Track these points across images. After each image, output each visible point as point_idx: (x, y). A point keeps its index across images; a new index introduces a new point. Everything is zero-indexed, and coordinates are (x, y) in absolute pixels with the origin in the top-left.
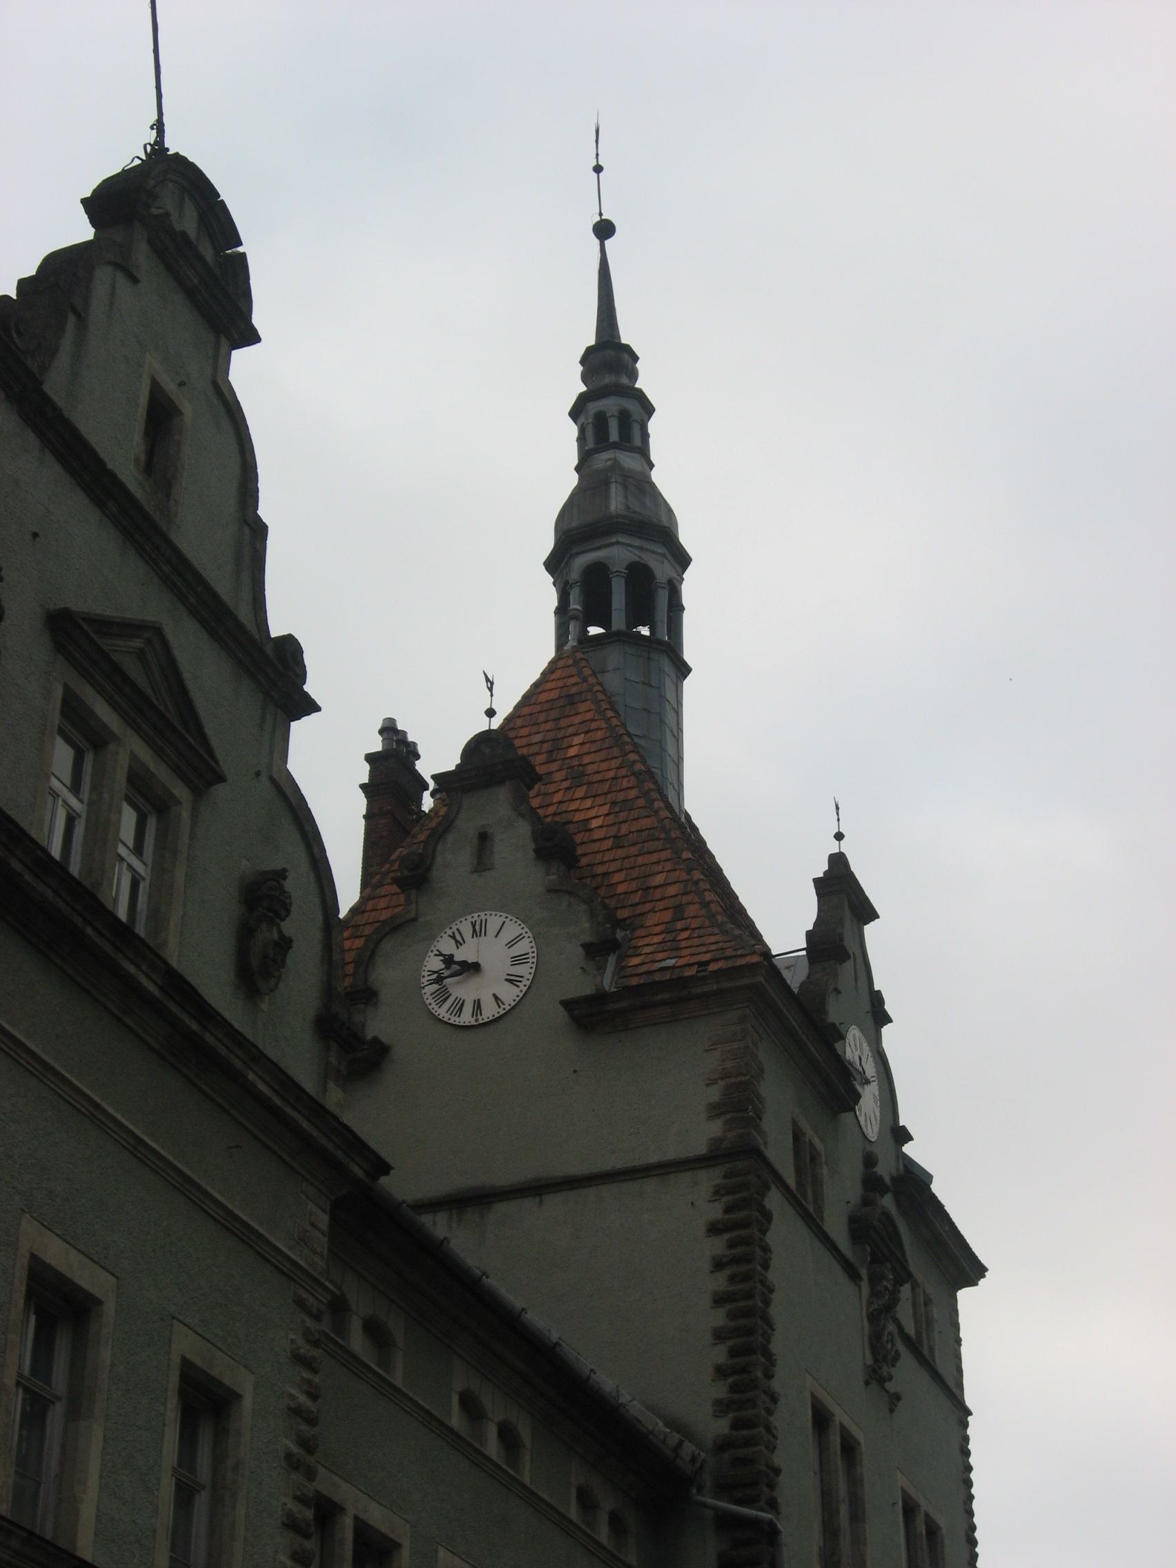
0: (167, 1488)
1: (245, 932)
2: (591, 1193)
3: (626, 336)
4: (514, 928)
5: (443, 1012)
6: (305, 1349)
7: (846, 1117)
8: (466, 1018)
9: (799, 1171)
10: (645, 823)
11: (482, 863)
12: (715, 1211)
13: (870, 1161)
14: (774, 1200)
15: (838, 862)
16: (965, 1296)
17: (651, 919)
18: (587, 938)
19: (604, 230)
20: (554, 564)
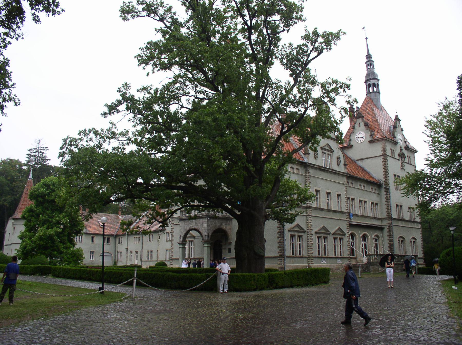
0: (337, 202)
1: (337, 161)
2: (372, 159)
3: (370, 54)
4: (363, 133)
5: (357, 141)
6: (346, 189)
7: (398, 145)
8: (360, 142)
9: (392, 153)
10: (375, 119)
11: (359, 126)
12: (383, 160)
13: (401, 147)
14: (388, 158)
15: (397, 116)
16: (415, 154)
17: (376, 131)
18: (370, 134)
19: (366, 38)
20: (365, 82)
